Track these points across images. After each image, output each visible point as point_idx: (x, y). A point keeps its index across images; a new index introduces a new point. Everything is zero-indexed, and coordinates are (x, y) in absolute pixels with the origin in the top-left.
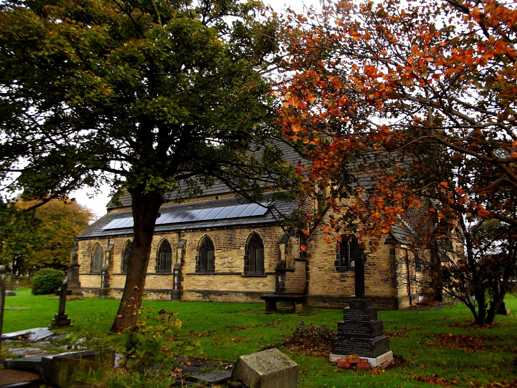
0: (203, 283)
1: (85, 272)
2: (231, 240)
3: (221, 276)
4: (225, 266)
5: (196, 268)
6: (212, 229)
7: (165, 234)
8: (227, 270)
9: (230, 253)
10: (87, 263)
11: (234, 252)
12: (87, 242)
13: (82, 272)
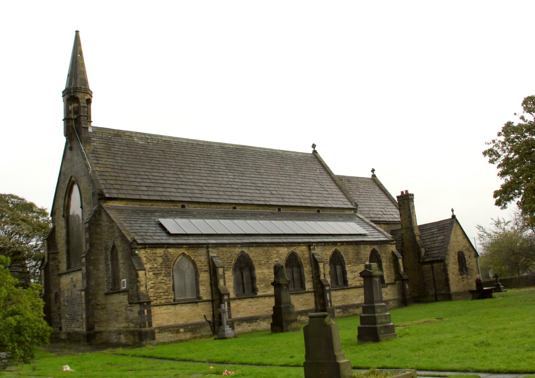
0: (340, 298)
1: (163, 301)
3: (355, 290)
4: (356, 279)
6: (342, 243)
7: (295, 246)
10: (165, 287)
12: (160, 251)
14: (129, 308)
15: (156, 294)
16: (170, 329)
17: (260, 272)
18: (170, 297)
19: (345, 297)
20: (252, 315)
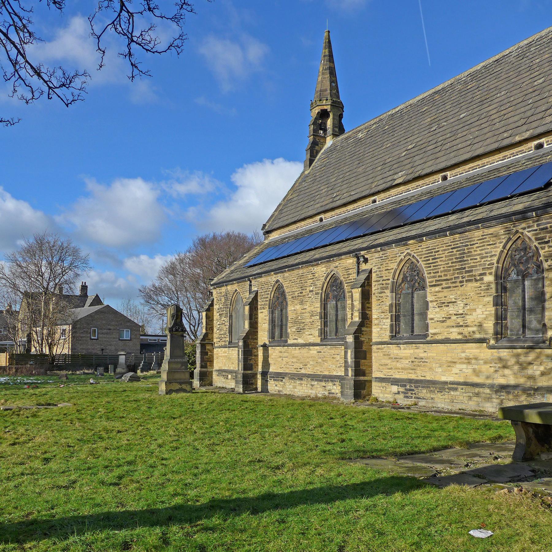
0: (405, 363)
2: (461, 260)
4: (449, 323)
5: (391, 332)
8: (454, 334)
13: (220, 344)
17: (293, 309)
19: (417, 362)
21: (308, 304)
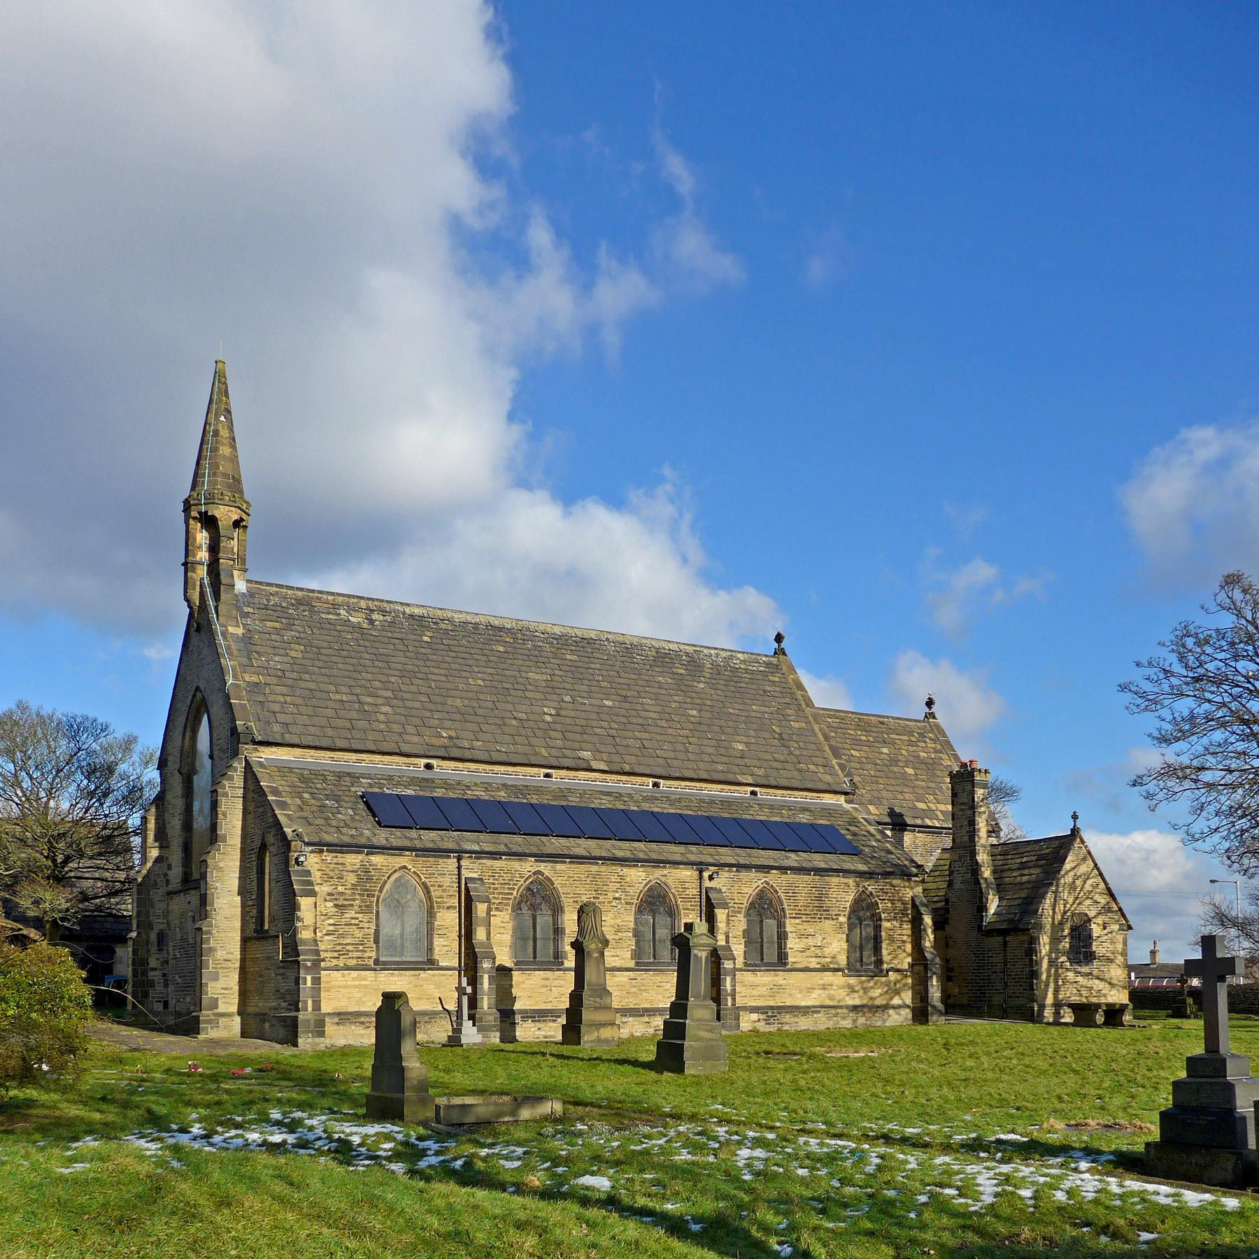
0: (763, 991)
1: (352, 962)
4: (808, 953)
8: (813, 964)
9: (818, 926)
10: (359, 934)
11: (828, 924)
12: (353, 860)
14: (281, 971)
15: (338, 948)
16: (362, 1019)
18: (366, 955)
19: (776, 989)
20: (549, 1007)
21: (611, 915)
